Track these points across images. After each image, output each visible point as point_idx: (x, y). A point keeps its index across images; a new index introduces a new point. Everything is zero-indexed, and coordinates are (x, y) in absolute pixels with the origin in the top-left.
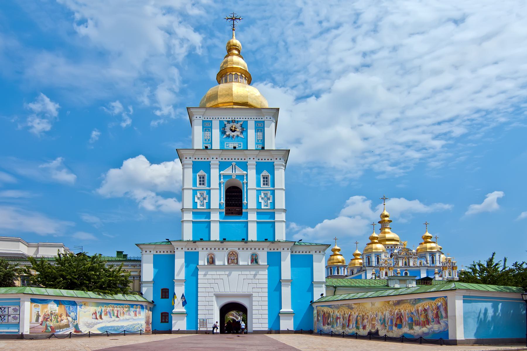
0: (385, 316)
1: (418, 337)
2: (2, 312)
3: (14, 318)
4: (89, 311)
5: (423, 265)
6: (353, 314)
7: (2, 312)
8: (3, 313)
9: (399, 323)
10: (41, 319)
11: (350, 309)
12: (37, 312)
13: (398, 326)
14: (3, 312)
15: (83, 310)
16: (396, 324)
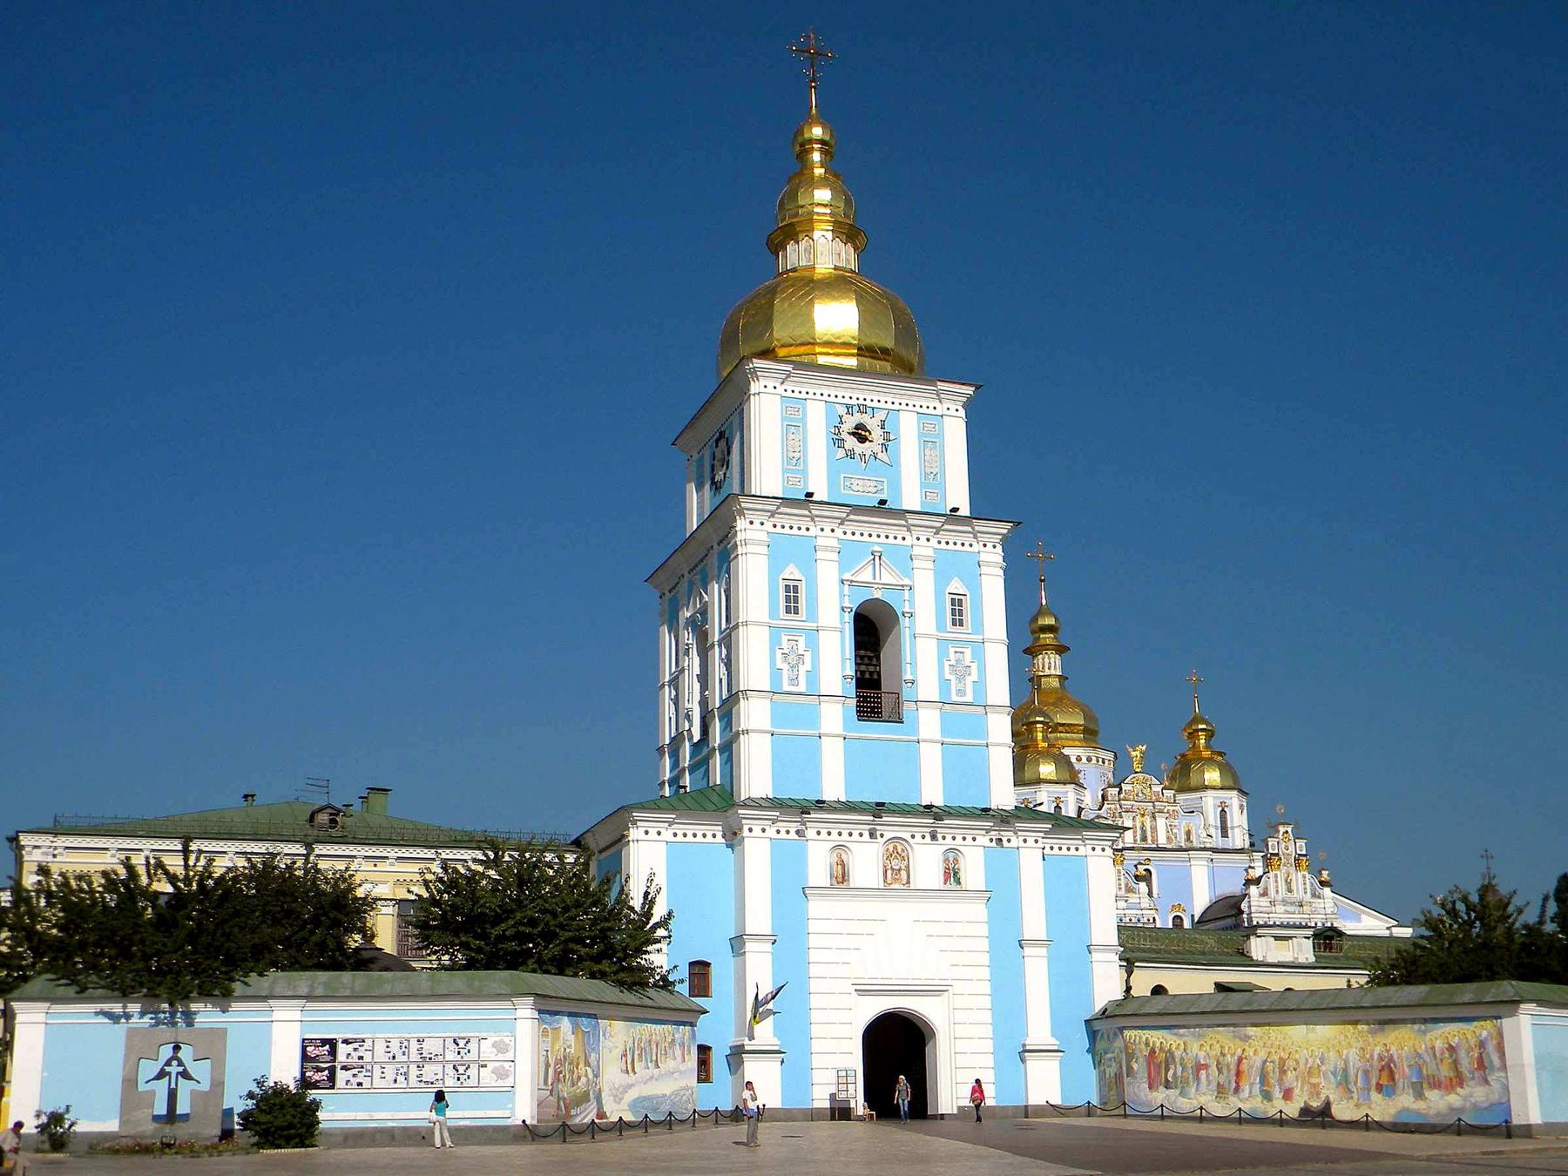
0: (1346, 1062)
1: (1452, 1120)
2: (459, 1053)
3: (501, 1074)
4: (617, 1047)
5: (1194, 841)
6: (1252, 1054)
7: (459, 1053)
8: (462, 1057)
9: (1386, 1083)
10: (551, 1071)
11: (1240, 1039)
12: (545, 1053)
13: (1384, 1089)
14: (462, 1052)
15: (608, 1043)
16: (1378, 1084)
